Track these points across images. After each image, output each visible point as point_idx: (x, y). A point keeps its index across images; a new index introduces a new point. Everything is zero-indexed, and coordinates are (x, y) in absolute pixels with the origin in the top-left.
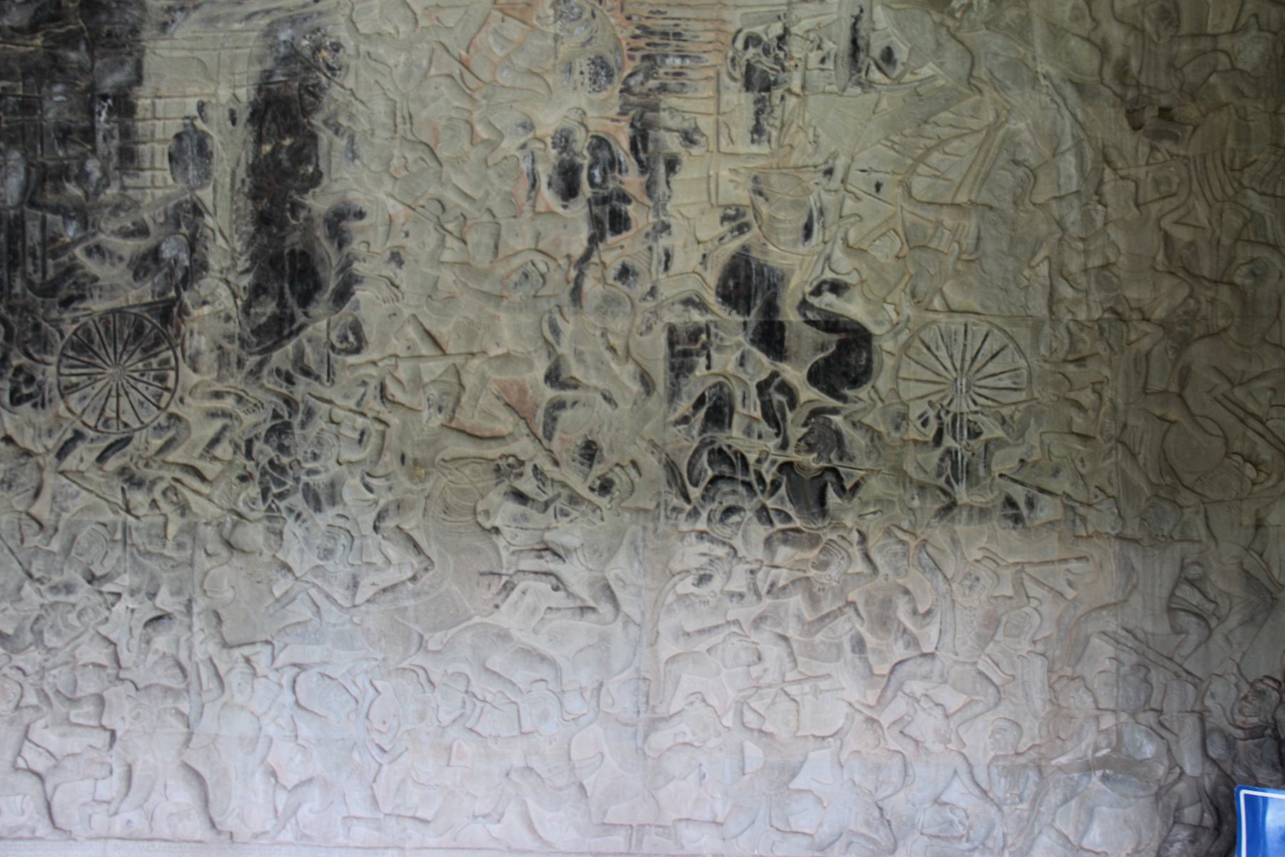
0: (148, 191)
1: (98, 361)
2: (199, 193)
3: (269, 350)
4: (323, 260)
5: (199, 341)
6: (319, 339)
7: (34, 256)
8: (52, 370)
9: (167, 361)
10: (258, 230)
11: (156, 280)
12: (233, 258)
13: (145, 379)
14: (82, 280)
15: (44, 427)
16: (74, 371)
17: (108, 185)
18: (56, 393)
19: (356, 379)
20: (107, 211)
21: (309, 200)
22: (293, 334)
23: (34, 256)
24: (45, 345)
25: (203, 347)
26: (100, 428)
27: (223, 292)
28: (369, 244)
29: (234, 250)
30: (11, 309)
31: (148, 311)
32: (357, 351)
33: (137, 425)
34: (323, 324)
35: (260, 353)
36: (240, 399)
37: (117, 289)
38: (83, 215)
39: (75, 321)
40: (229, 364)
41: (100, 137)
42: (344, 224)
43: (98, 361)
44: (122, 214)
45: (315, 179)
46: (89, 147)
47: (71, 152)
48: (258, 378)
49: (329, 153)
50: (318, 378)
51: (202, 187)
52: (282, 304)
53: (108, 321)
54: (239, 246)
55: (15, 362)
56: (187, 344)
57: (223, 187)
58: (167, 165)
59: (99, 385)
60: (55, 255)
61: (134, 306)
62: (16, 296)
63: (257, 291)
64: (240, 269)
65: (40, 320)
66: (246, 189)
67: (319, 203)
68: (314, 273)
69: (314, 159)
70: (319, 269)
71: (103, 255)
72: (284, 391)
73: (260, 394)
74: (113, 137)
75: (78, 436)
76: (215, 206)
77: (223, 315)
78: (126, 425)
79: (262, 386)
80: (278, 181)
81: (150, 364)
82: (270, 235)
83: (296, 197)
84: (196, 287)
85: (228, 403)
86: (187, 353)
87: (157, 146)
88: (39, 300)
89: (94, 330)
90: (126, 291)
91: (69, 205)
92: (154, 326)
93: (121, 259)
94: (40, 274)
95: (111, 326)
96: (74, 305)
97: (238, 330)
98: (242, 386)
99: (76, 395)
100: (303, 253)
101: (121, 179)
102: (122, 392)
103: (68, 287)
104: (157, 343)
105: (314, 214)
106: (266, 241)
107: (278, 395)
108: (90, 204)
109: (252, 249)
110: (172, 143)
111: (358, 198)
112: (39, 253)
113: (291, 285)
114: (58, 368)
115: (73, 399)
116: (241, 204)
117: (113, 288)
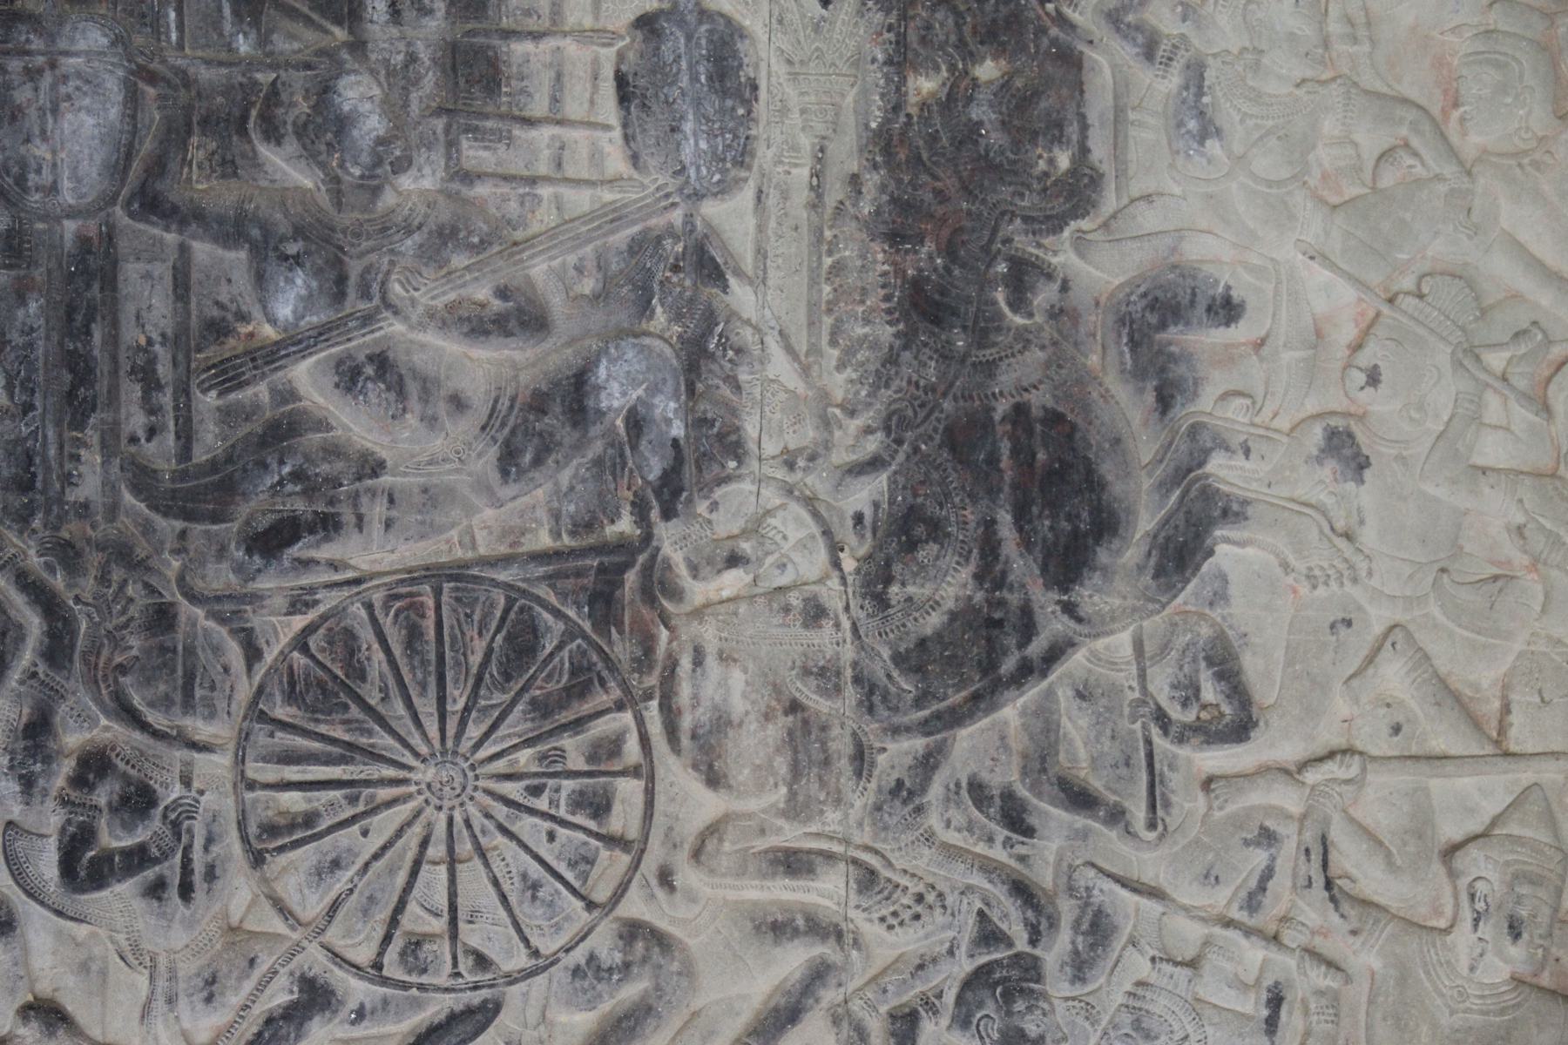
0: (545, 191)
1: (383, 740)
2: (711, 209)
3: (954, 718)
4: (1117, 441)
5: (723, 683)
6: (1115, 690)
7: (150, 383)
8: (215, 767)
9: (613, 746)
10: (907, 339)
11: (565, 477)
12: (826, 423)
13: (542, 804)
14: (324, 468)
15: (188, 967)
16: (292, 773)
18: (231, 844)
19: (1237, 822)
21: (1061, 253)
22: (1026, 671)
23: (150, 383)
24: (189, 688)
25: (738, 706)
26: (392, 970)
27: (792, 526)
28: (1254, 402)
29: (824, 396)
30: (67, 554)
31: (550, 578)
32: (1241, 730)
33: (521, 960)
34: (1121, 642)
35: (926, 728)
36: (868, 880)
37: (446, 501)
38: (325, 249)
39: (298, 604)
40: (826, 763)
42: (1175, 335)
43: (383, 740)
44: (459, 260)
45: (1079, 192)
46: (340, 34)
47: (281, 44)
48: (919, 810)
49: (1119, 111)
50: (1116, 816)
51: (723, 189)
52: (990, 573)
53: (420, 610)
54: (839, 384)
55: (73, 738)
56: (685, 692)
57: (785, 196)
59: (384, 824)
60: (228, 377)
61: (506, 561)
62: (84, 508)
63: (906, 531)
64: (841, 457)
65: (172, 594)
66: (866, 208)
67: (1094, 266)
68: (1094, 483)
69: (1073, 131)
70: (1107, 469)
71: (400, 390)
72: (999, 854)
73: (924, 860)
75: (315, 997)
76: (761, 253)
77: (795, 599)
78: (482, 962)
79: (929, 838)
80: (967, 190)
81: (561, 754)
82: (945, 355)
83: (1024, 244)
84: (702, 507)
85: (827, 891)
86: (686, 722)
87: (570, 47)
88: (168, 526)
89: (366, 635)
90: (470, 510)
91: (284, 228)
92: (572, 632)
93: (458, 403)
94: (170, 440)
95: (429, 624)
96: (295, 551)
97: (848, 653)
98: (865, 836)
99: (307, 855)
100: (1054, 418)
101: (452, 144)
102: (465, 847)
103: (276, 492)
104: (581, 682)
105: (1080, 297)
106: (932, 373)
107: (988, 868)
108: (347, 218)
109: (886, 394)
111: (1215, 255)
112: (164, 370)
113: (1021, 515)
114: (240, 760)
115: (293, 871)
116: (848, 253)
117: (431, 497)
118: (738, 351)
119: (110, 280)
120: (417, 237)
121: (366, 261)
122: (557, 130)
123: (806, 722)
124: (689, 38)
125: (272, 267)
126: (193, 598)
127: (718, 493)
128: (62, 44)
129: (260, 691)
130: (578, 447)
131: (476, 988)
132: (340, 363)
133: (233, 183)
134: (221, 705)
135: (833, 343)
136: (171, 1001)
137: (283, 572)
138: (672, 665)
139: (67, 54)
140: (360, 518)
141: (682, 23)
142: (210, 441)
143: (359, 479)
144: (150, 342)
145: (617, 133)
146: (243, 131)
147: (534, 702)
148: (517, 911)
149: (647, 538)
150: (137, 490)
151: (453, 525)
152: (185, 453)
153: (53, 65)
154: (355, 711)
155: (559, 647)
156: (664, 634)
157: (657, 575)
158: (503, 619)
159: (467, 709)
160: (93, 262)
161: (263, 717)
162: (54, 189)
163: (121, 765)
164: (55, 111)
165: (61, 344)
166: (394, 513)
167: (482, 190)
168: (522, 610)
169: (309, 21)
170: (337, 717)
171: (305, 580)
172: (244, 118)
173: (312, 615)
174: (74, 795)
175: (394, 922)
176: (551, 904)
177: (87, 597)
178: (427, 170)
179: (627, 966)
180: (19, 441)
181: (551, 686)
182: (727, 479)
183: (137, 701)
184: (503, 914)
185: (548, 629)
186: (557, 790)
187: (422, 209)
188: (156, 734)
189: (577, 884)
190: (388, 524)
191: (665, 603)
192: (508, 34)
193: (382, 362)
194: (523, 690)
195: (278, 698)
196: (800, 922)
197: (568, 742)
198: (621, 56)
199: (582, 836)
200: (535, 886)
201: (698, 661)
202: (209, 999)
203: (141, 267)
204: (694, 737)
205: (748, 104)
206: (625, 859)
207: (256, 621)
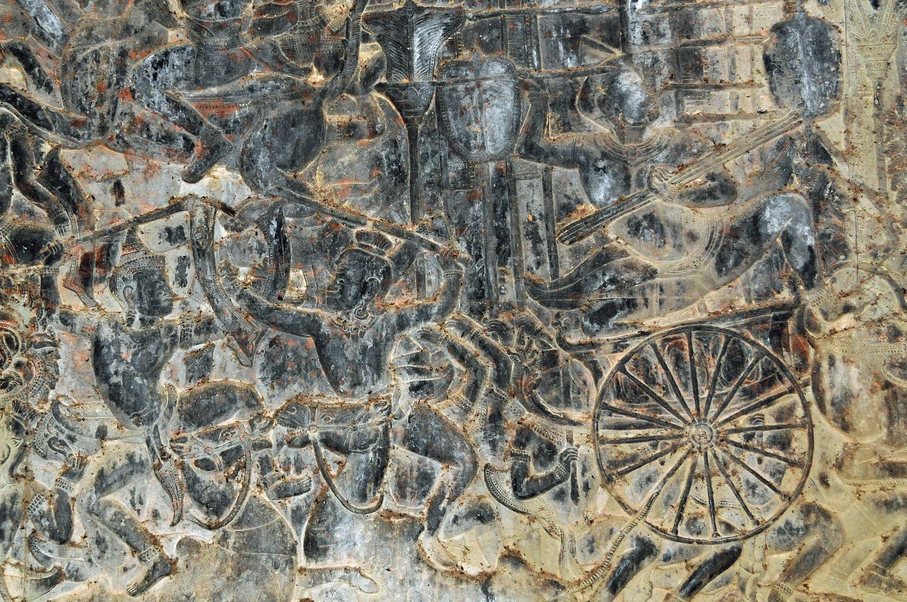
1: (667, 415)
5: (847, 375)
11: (751, 271)
14: (626, 276)
16: (622, 434)
17: (654, 117)
18: (595, 470)
20: (661, 157)
25: (856, 386)
26: (683, 533)
31: (749, 325)
33: (750, 527)
39: (619, 346)
41: (636, 36)
43: (667, 415)
46: (618, 53)
51: (826, 112)
56: (826, 381)
58: (761, 79)
60: (574, 234)
62: (509, 306)
65: (555, 346)
71: (661, 231)
74: (661, 35)
75: (645, 550)
78: (729, 528)
81: (762, 417)
86: (828, 397)
89: (654, 360)
90: (703, 293)
92: (763, 352)
95: (686, 353)
96: (614, 320)
101: (679, 102)
108: (628, 146)
110: (768, 39)
112: (542, 233)
118: (841, 196)
119: (513, 192)
120: (665, 153)
121: (639, 167)
122: (734, 90)
123: (894, 393)
124: (802, 33)
125: (593, 175)
126: (567, 347)
127: (835, 274)
128: (482, 75)
129: (603, 392)
130: (758, 255)
131: (728, 541)
132: (630, 221)
133: (570, 134)
134: (583, 400)
135: (894, 188)
136: (573, 552)
137: (610, 331)
138: (818, 366)
139: (485, 79)
140: (646, 300)
141: (798, 26)
142: (567, 268)
143: (644, 280)
144: (534, 219)
145: (766, 88)
146: (572, 107)
147: (744, 390)
148: (745, 501)
149: (798, 300)
150: (534, 294)
151: (694, 301)
152: (555, 275)
153: (479, 86)
154: (651, 401)
155: (756, 361)
156: (812, 351)
157: (805, 318)
158: (725, 348)
159: (710, 396)
160: (505, 181)
161: (606, 407)
162: (483, 147)
163: (537, 434)
164: (481, 108)
165: (491, 224)
166: (664, 297)
167: (696, 125)
168: (734, 342)
169: (602, 48)
170: (643, 404)
171: (621, 335)
172: (573, 101)
173: (626, 352)
174: (515, 450)
175: (682, 508)
176: (763, 496)
177: (513, 350)
178: (667, 117)
179: (807, 527)
180: (475, 274)
181: (754, 382)
182: (840, 266)
183: (542, 401)
184: (738, 502)
185: (749, 351)
186: (761, 436)
187: (666, 137)
188: (554, 418)
189: (775, 485)
190: (661, 302)
191: (811, 334)
192: (706, 43)
193: (651, 218)
194: (740, 384)
195: (612, 396)
196: (900, 500)
197: (764, 411)
198: (766, 48)
199: (776, 460)
200: (753, 487)
201: (832, 363)
202: (592, 551)
203: (528, 182)
204: (833, 404)
205: (836, 64)
206: (799, 472)
207: (598, 356)
